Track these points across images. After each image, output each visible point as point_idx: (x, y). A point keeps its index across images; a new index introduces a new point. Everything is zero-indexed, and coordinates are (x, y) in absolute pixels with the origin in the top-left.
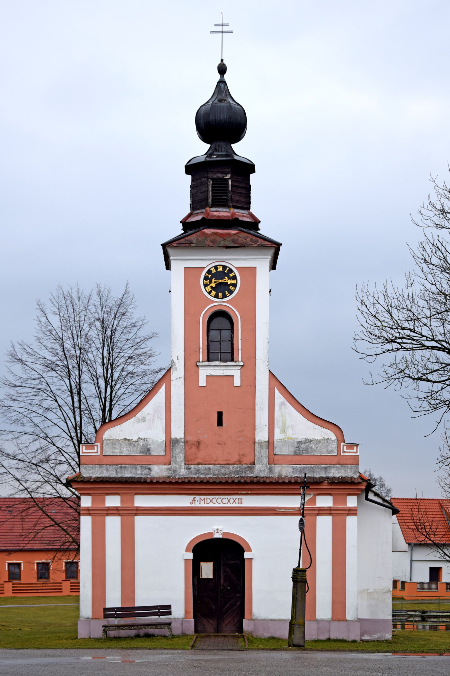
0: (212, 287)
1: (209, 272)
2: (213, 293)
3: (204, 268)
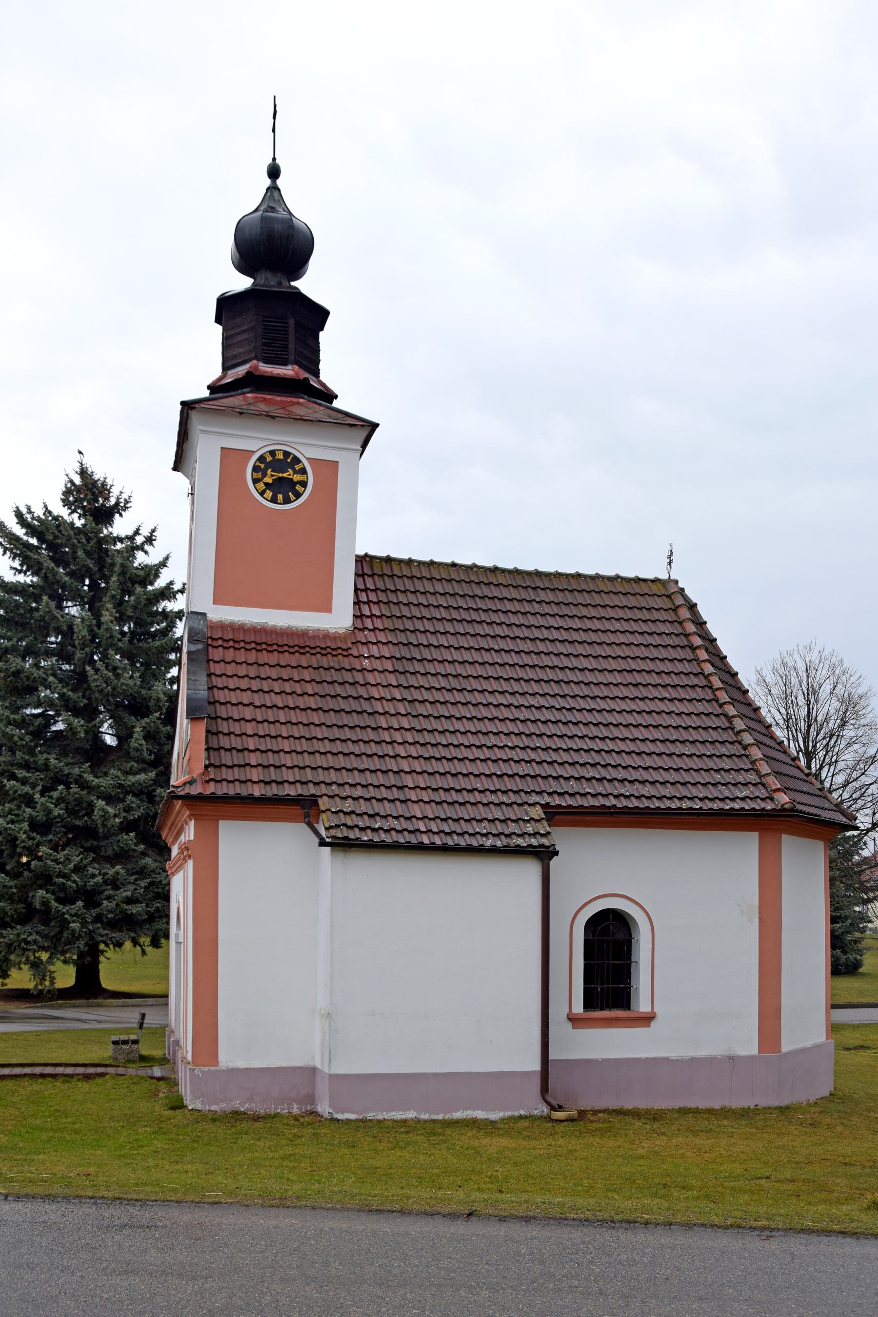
0: (266, 484)
1: (262, 459)
2: (269, 494)
3: (254, 452)
